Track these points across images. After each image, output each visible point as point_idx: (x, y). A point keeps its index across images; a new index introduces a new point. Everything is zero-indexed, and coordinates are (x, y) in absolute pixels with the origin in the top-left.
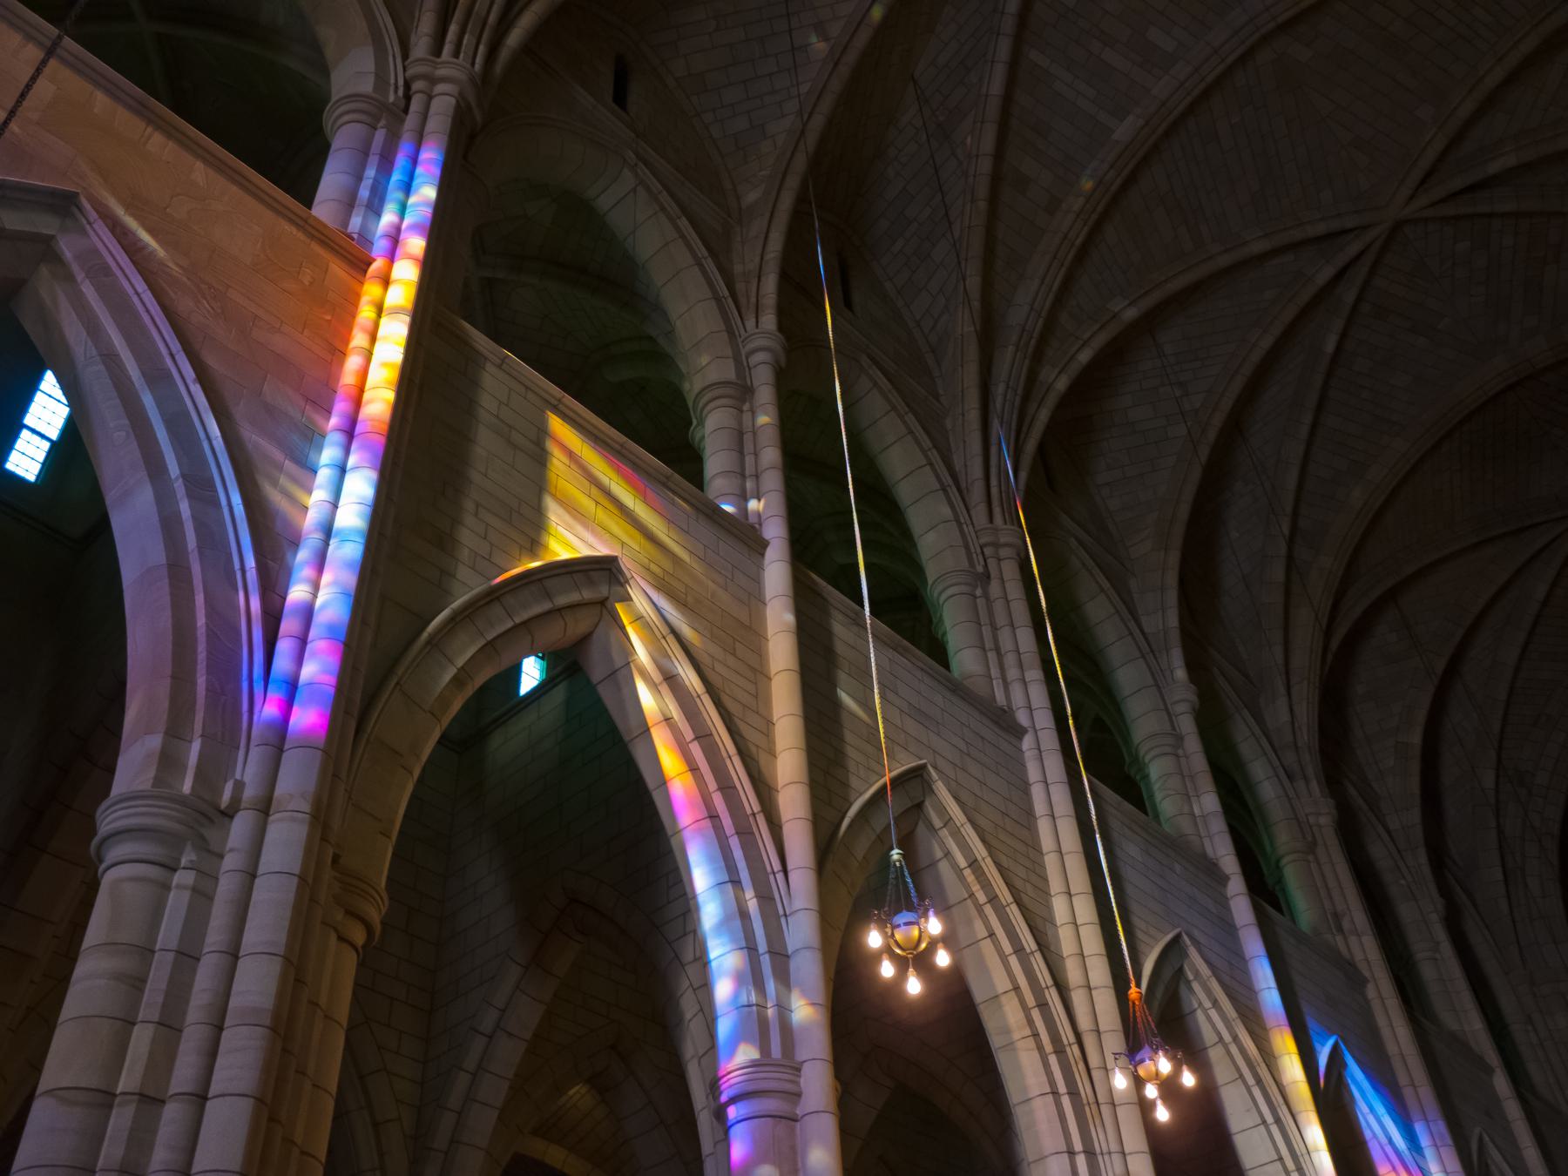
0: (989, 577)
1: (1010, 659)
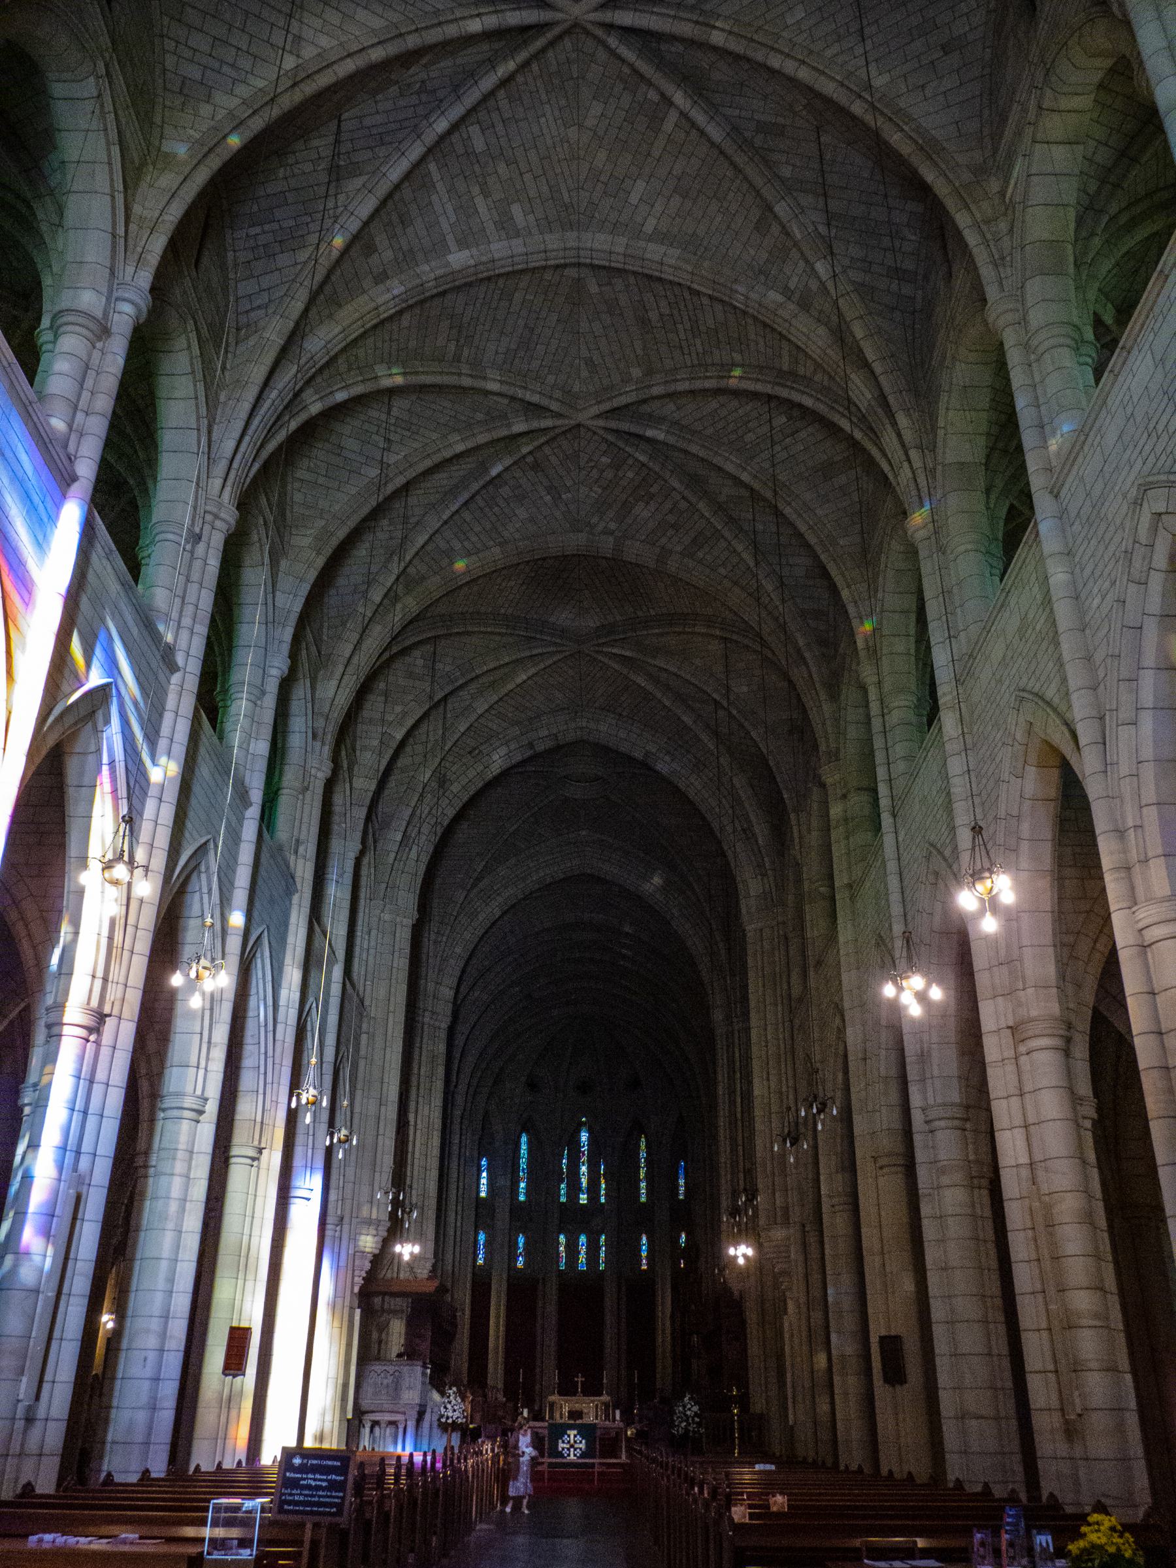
0: (200, 538)
1: (189, 610)
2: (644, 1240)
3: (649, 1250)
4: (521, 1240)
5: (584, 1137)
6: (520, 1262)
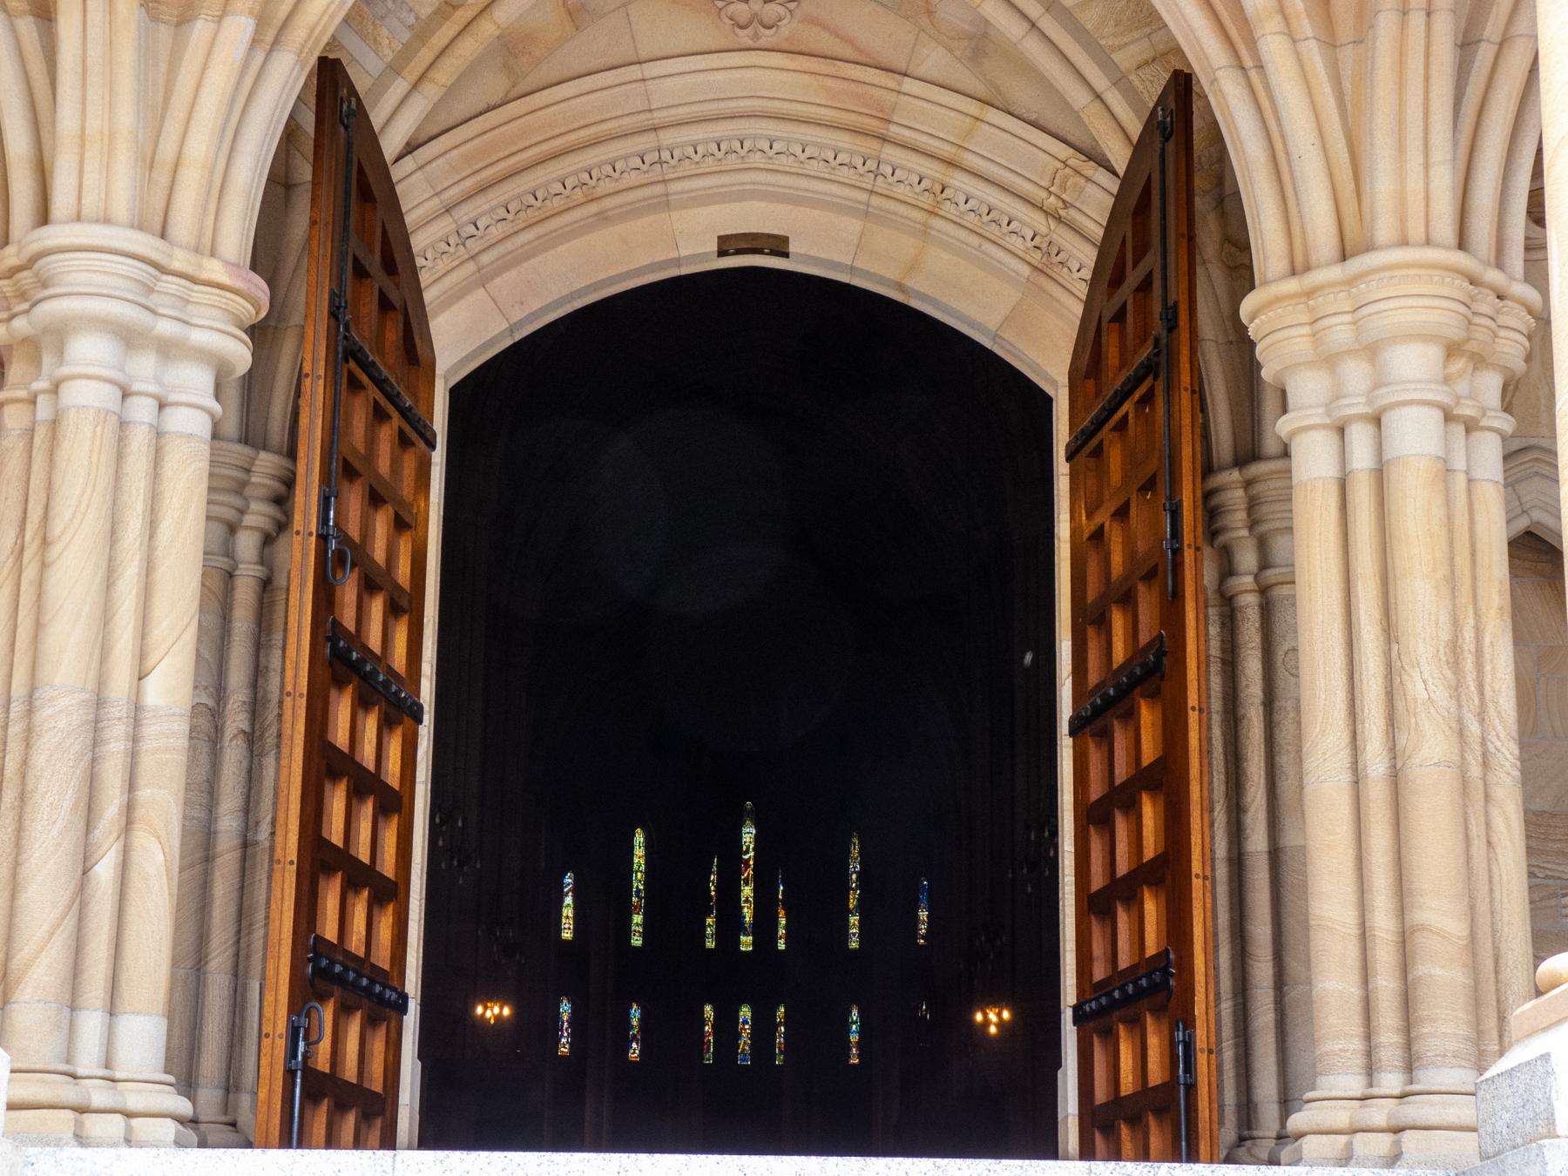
2: (855, 1015)
3: (861, 1032)
4: (635, 1014)
5: (748, 835)
6: (634, 1052)
